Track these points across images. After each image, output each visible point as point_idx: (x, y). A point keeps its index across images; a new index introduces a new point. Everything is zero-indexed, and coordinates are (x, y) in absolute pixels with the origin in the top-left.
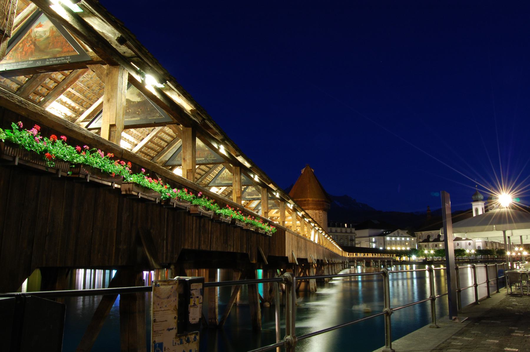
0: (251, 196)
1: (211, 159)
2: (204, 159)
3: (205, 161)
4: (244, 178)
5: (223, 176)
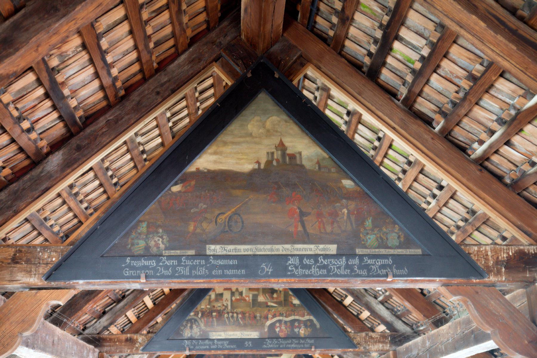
1: (383, 251)
2: (333, 249)
3: (343, 261)
4: (312, 317)
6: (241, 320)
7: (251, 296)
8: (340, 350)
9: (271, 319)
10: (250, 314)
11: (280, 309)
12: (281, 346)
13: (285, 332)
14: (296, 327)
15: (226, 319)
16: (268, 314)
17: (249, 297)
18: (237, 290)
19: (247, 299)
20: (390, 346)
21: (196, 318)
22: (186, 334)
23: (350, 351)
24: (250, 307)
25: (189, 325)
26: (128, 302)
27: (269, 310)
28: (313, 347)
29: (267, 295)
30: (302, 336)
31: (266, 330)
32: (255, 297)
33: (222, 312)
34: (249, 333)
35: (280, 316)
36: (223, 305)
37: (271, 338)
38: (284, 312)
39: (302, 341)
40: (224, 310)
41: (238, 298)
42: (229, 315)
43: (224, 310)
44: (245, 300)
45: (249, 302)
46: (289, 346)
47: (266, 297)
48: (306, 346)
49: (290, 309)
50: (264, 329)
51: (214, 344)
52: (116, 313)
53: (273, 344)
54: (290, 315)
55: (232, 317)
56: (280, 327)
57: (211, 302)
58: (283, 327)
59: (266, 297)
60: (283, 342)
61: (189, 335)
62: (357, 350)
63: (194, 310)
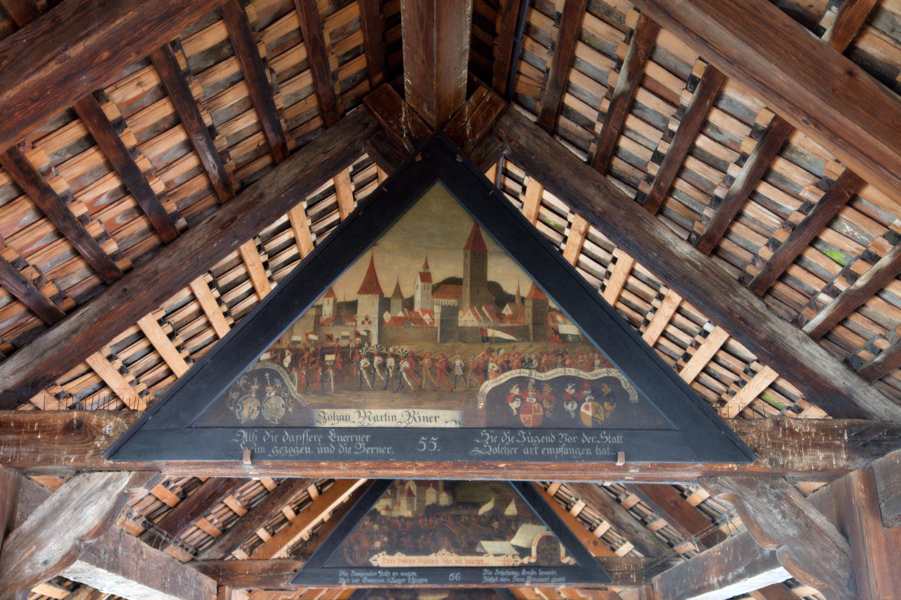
0: (409, 552)
4: (615, 373)
5: (342, 334)
6: (409, 376)
7: (437, 310)
8: (699, 465)
9: (495, 377)
10: (433, 360)
11: (522, 347)
12: (526, 452)
13: (536, 411)
14: (571, 399)
15: (364, 372)
16: (486, 363)
17: (431, 313)
18: (398, 292)
19: (426, 317)
20: (848, 459)
21: (275, 366)
22: (245, 413)
23: (731, 473)
24: (434, 340)
25: (255, 387)
26: (81, 324)
27: (490, 351)
28: (621, 455)
29: (483, 308)
30: (588, 423)
31: (481, 405)
32: (450, 315)
33: (353, 354)
34: (430, 413)
35: (522, 367)
36: (357, 334)
37: (496, 429)
38: (534, 356)
39: (586, 439)
40: (360, 346)
41: (401, 314)
42: (372, 362)
43: (360, 346)
44: (421, 321)
45: (432, 327)
46: (550, 451)
47: (483, 314)
48: (599, 451)
49: (551, 350)
50: (476, 402)
51: (326, 442)
52: (45, 352)
53: (502, 445)
54: (551, 366)
55: (383, 366)
56: (522, 397)
57: (322, 325)
58: (531, 399)
59: (483, 314)
60: (533, 441)
61: (254, 416)
62: (750, 466)
63: (271, 345)
